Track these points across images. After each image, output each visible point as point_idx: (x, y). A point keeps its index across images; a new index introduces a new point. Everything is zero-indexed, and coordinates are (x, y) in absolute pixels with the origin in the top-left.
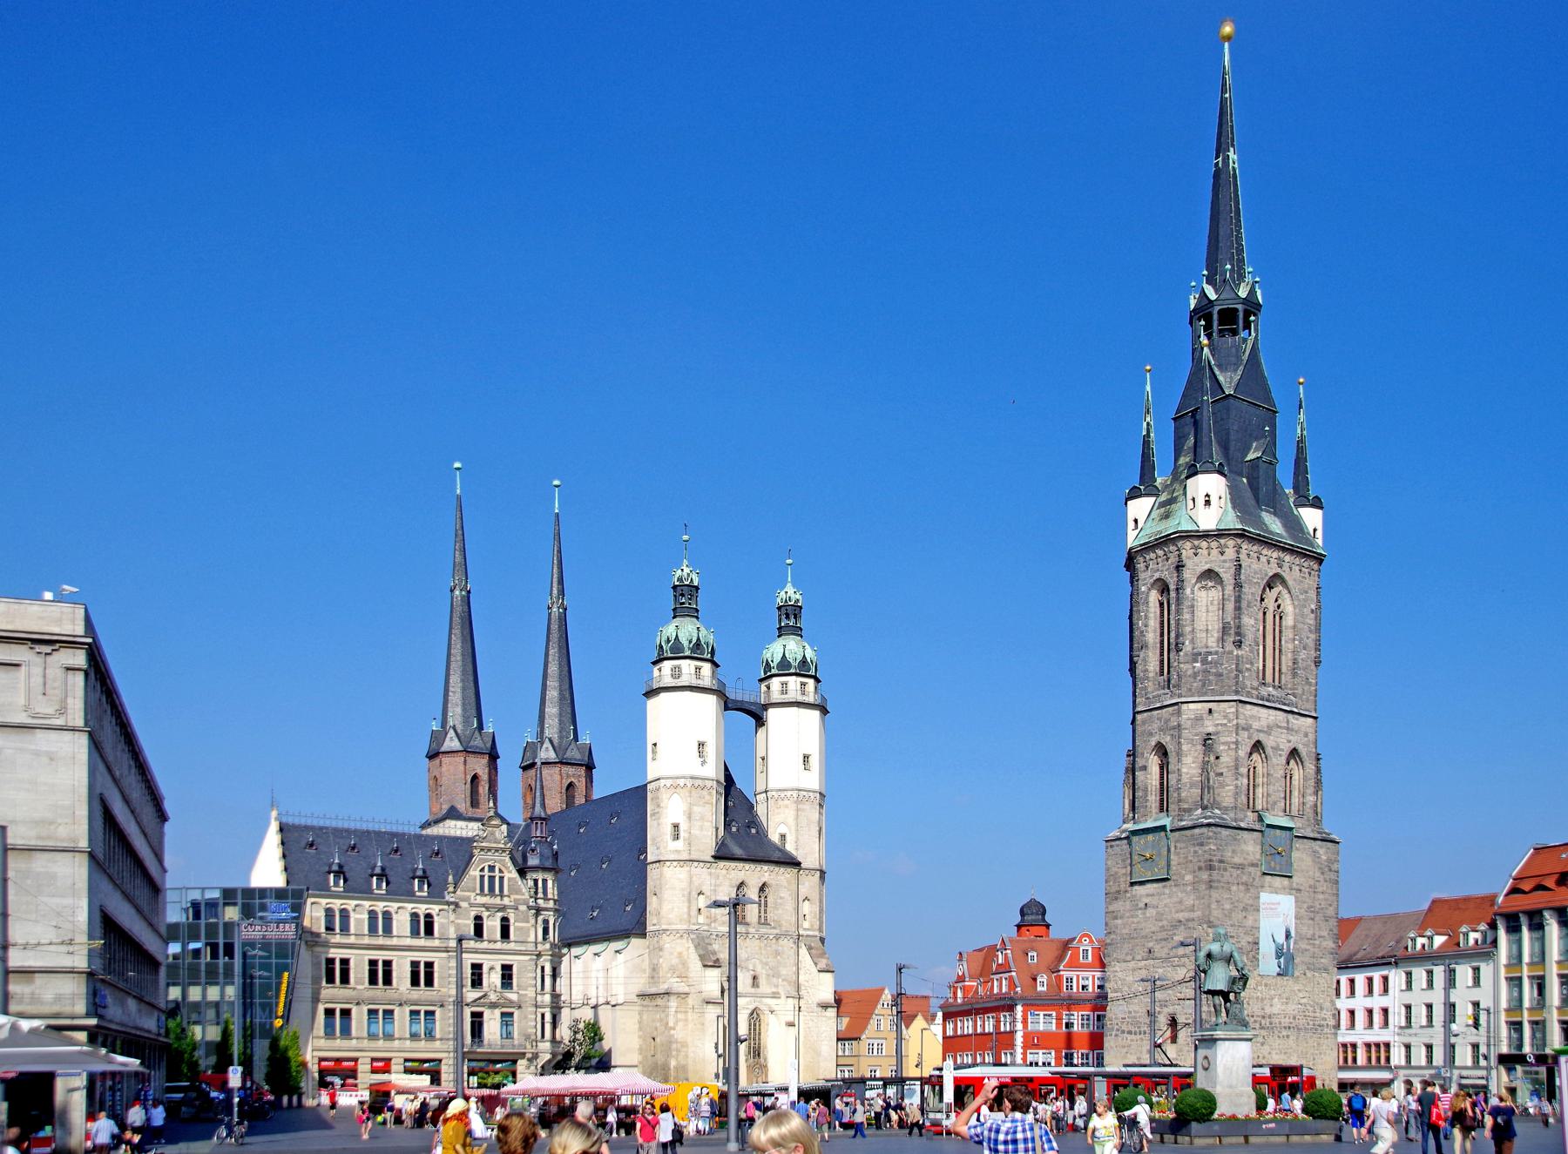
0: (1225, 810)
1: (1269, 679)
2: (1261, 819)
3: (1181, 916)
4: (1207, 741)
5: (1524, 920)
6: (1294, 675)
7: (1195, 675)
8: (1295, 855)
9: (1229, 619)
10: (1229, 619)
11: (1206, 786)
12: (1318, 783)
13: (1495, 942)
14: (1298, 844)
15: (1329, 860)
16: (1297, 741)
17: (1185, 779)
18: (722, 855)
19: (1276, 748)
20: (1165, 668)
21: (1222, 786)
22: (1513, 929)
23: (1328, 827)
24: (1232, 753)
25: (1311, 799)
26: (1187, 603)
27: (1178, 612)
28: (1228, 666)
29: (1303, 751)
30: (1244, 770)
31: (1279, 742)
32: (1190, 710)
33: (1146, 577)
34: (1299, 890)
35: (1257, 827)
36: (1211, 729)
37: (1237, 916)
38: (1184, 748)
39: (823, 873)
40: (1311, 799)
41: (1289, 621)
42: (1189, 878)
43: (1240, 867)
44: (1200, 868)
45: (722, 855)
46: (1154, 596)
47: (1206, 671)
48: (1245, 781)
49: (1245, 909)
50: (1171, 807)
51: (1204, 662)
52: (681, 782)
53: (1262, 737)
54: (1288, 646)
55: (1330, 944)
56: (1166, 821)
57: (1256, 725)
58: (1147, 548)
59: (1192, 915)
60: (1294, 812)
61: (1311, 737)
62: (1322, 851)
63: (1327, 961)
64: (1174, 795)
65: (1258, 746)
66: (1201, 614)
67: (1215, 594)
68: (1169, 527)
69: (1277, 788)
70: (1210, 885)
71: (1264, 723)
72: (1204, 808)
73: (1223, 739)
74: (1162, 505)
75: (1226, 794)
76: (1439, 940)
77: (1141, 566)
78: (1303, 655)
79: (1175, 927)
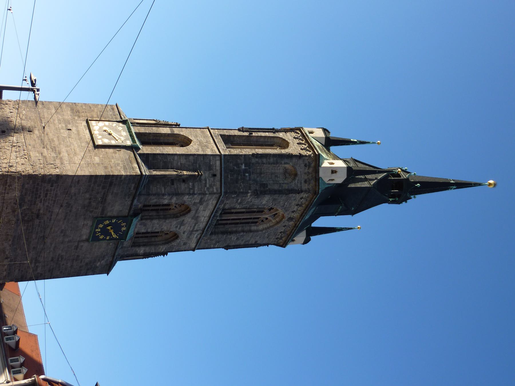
3: (64, 154)
7: (238, 165)
9: (269, 187)
24: (187, 191)
34: (77, 247)
42: (97, 160)
44: (106, 168)
48: (166, 202)
51: (245, 171)
53: (193, 213)
57: (201, 208)
62: (103, 262)
73: (196, 184)
78: (234, 237)
79: (54, 149)
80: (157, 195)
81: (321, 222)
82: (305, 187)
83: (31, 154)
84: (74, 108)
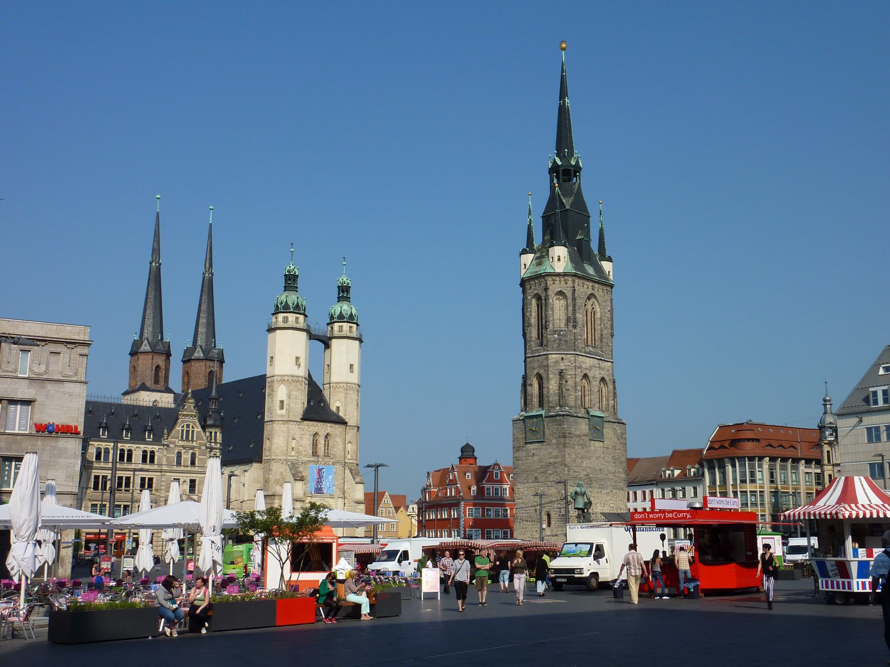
0: (571, 407)
1: (590, 343)
2: (588, 412)
3: (551, 460)
4: (561, 373)
5: (716, 463)
6: (601, 341)
7: (555, 341)
8: (605, 430)
9: (570, 315)
10: (570, 315)
11: (561, 395)
12: (615, 394)
13: (703, 475)
14: (606, 425)
15: (621, 433)
16: (604, 373)
17: (551, 392)
18: (308, 417)
19: (594, 377)
20: (541, 336)
21: (569, 395)
22: (711, 469)
23: (621, 416)
25: (611, 402)
26: (550, 306)
27: (546, 310)
28: (570, 337)
29: (607, 379)
30: (579, 388)
31: (595, 374)
32: (553, 358)
33: (531, 292)
35: (586, 416)
36: (563, 368)
37: (579, 461)
38: (550, 376)
39: (358, 428)
40: (611, 402)
41: (598, 315)
42: (554, 441)
43: (579, 436)
45: (308, 417)
46: (534, 302)
47: (560, 339)
49: (582, 458)
50: (545, 405)
51: (559, 335)
52: (286, 378)
53: (587, 372)
54: (598, 328)
55: (623, 476)
56: (543, 412)
57: (584, 366)
58: (531, 279)
59: (556, 460)
60: (604, 409)
61: (611, 371)
63: (622, 484)
64: (545, 400)
65: (585, 376)
66: (557, 311)
67: (563, 302)
68: (542, 270)
69: (595, 397)
70: (565, 446)
71: (588, 365)
72: (561, 406)
74: (537, 258)
75: (571, 399)
76: (677, 472)
77: (528, 287)
78: (605, 332)
80: (576, 400)
81: (594, 246)
82: (570, 283)
83: (551, 479)
84: (516, 449)
